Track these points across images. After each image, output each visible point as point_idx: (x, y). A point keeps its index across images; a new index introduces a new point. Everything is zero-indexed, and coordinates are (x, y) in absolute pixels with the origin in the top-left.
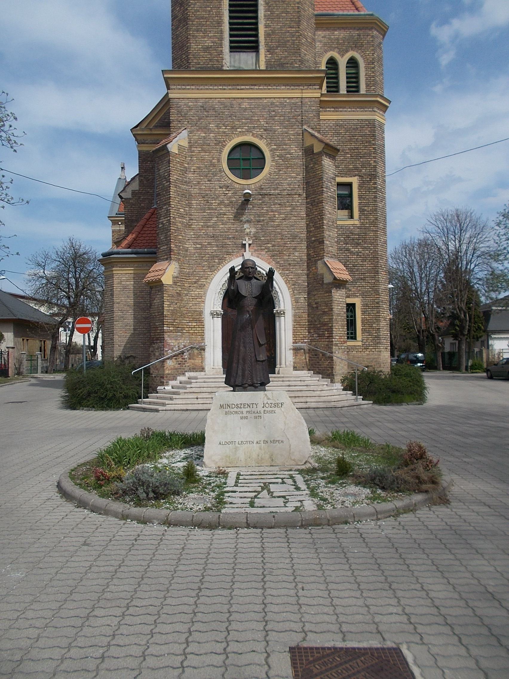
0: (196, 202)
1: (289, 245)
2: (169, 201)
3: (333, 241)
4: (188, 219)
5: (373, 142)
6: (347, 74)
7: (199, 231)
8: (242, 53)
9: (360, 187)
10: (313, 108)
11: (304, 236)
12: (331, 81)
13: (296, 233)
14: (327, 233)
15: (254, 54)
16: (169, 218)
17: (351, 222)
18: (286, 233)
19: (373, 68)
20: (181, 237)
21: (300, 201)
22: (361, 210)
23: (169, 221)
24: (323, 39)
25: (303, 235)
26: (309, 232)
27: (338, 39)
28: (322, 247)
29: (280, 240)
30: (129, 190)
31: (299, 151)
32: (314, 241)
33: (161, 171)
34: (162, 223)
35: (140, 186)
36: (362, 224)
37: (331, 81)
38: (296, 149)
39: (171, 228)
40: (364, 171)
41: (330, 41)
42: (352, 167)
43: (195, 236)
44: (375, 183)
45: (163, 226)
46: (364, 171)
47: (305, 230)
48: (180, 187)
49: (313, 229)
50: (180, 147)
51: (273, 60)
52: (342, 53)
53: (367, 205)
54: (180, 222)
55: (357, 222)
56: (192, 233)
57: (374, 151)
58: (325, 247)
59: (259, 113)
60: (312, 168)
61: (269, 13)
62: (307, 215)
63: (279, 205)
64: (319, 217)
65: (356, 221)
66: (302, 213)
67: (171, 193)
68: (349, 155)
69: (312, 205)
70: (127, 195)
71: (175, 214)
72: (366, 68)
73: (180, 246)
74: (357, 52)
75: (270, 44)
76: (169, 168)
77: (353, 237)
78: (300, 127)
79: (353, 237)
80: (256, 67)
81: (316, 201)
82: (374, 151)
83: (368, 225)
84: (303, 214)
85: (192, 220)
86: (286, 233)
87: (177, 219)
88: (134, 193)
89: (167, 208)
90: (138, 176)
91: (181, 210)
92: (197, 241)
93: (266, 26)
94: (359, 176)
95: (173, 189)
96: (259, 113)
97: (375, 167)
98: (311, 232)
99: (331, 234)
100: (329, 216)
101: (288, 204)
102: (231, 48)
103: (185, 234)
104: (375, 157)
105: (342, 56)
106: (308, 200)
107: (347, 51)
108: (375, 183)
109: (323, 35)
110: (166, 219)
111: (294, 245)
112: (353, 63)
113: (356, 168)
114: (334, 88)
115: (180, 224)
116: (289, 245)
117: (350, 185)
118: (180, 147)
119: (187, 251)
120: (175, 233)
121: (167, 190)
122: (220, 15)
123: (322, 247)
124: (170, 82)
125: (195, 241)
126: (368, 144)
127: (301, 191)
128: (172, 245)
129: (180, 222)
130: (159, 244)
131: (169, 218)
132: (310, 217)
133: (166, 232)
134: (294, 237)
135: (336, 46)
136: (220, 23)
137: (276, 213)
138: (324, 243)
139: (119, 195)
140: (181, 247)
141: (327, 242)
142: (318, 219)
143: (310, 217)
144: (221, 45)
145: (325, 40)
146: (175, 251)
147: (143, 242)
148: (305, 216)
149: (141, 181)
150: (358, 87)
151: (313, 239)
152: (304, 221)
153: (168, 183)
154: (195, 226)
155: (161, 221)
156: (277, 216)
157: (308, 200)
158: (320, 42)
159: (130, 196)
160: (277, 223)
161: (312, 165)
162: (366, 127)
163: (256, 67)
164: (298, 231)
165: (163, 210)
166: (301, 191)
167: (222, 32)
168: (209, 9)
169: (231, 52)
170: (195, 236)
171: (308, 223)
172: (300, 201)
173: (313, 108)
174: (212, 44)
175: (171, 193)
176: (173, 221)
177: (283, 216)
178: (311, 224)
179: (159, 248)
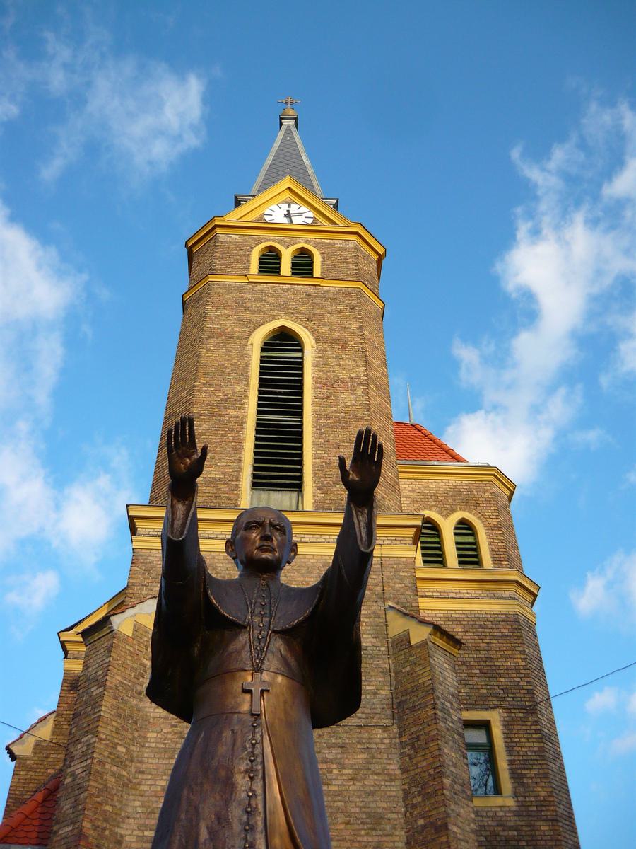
0: (155, 735)
1: (365, 839)
2: (97, 724)
3: (467, 828)
4: (133, 770)
5: (521, 649)
6: (457, 543)
7: (154, 799)
8: (272, 493)
9: (508, 729)
10: (403, 574)
11: (397, 817)
12: (429, 552)
13: (379, 810)
14: (453, 806)
15: (294, 495)
16: (89, 762)
17: (499, 801)
18: (357, 810)
19: (500, 535)
20: (109, 808)
21: (386, 741)
22: (516, 777)
23: (89, 767)
24: (412, 494)
25: (395, 816)
26: (410, 807)
27: (435, 495)
28: (444, 839)
29: (342, 827)
30: (30, 742)
31: (379, 644)
32: (424, 827)
33: (90, 669)
34: (73, 774)
35: (54, 733)
36: (522, 805)
37: (429, 552)
38: (374, 640)
39: (91, 783)
40: (509, 699)
41: (423, 497)
42: (485, 691)
43: (144, 810)
44: (536, 723)
45: (74, 780)
46: (509, 699)
47: (401, 803)
48: (125, 702)
49: (420, 799)
50: (137, 628)
51: (328, 502)
52: (447, 513)
53: (526, 764)
54: (113, 774)
55: (510, 802)
56: (137, 803)
57: (524, 664)
58: (451, 839)
59: (301, 579)
60: (408, 673)
61: (323, 441)
62: (404, 770)
63: (342, 747)
64: (432, 771)
65: (507, 801)
66: (392, 767)
67: (103, 708)
68: (478, 671)
69: (413, 747)
70: (24, 750)
71: (106, 754)
72: (490, 535)
73: (104, 829)
74: (471, 513)
75: (322, 479)
76: (107, 660)
77: (506, 833)
78: (380, 603)
79: (506, 833)
80: (297, 507)
81: (422, 738)
82: (524, 664)
83: (535, 808)
84: (394, 767)
85: (143, 772)
86: (357, 810)
87: (107, 766)
88: (38, 747)
89: (89, 740)
90: (54, 715)
91: (119, 748)
92: (147, 822)
93: (315, 457)
94: (503, 708)
95: (108, 701)
96: (301, 579)
97: (531, 692)
98: (414, 806)
99: (462, 811)
100: (453, 769)
101: (359, 746)
102: (254, 484)
103: (121, 802)
104: (527, 675)
105: (446, 516)
106: (405, 739)
107: (453, 511)
108: (538, 722)
109: (410, 489)
110: (82, 765)
111: (376, 839)
112: (464, 527)
113: (496, 695)
114: (434, 556)
115: (112, 779)
116: (365, 839)
117: (485, 725)
118: (137, 628)
119: (119, 843)
120: (98, 797)
121: (96, 703)
122: (239, 442)
123: (444, 839)
124: (138, 523)
125: (143, 821)
126: (510, 652)
127: (387, 722)
128: (85, 824)
129: (113, 774)
130: (58, 823)
131: (89, 762)
132: (412, 773)
133: (77, 792)
134: (375, 820)
135: (433, 503)
136: (238, 450)
137: (335, 766)
138: (447, 829)
139: (8, 748)
140: (107, 833)
141: (455, 829)
142: (430, 775)
143: (412, 773)
144: (237, 478)
145: (415, 496)
146: (91, 839)
147: (29, 835)
148: (398, 772)
149: (57, 725)
150: (478, 564)
151: (421, 822)
152: (397, 783)
153: (101, 689)
154: (146, 788)
155: (72, 769)
156: (335, 772)
157: (405, 739)
158: (407, 497)
159: (29, 752)
160: (335, 788)
161: (408, 669)
162: (503, 623)
163: (297, 507)
164: (385, 805)
165: (79, 746)
166: (387, 722)
167: (240, 461)
168: (223, 432)
169: (252, 489)
170: (144, 810)
171: (406, 787)
172: (386, 741)
173: (403, 574)
174: (222, 476)
175: (103, 708)
176: (98, 767)
177: (350, 772)
178: (413, 790)
179: (56, 832)
